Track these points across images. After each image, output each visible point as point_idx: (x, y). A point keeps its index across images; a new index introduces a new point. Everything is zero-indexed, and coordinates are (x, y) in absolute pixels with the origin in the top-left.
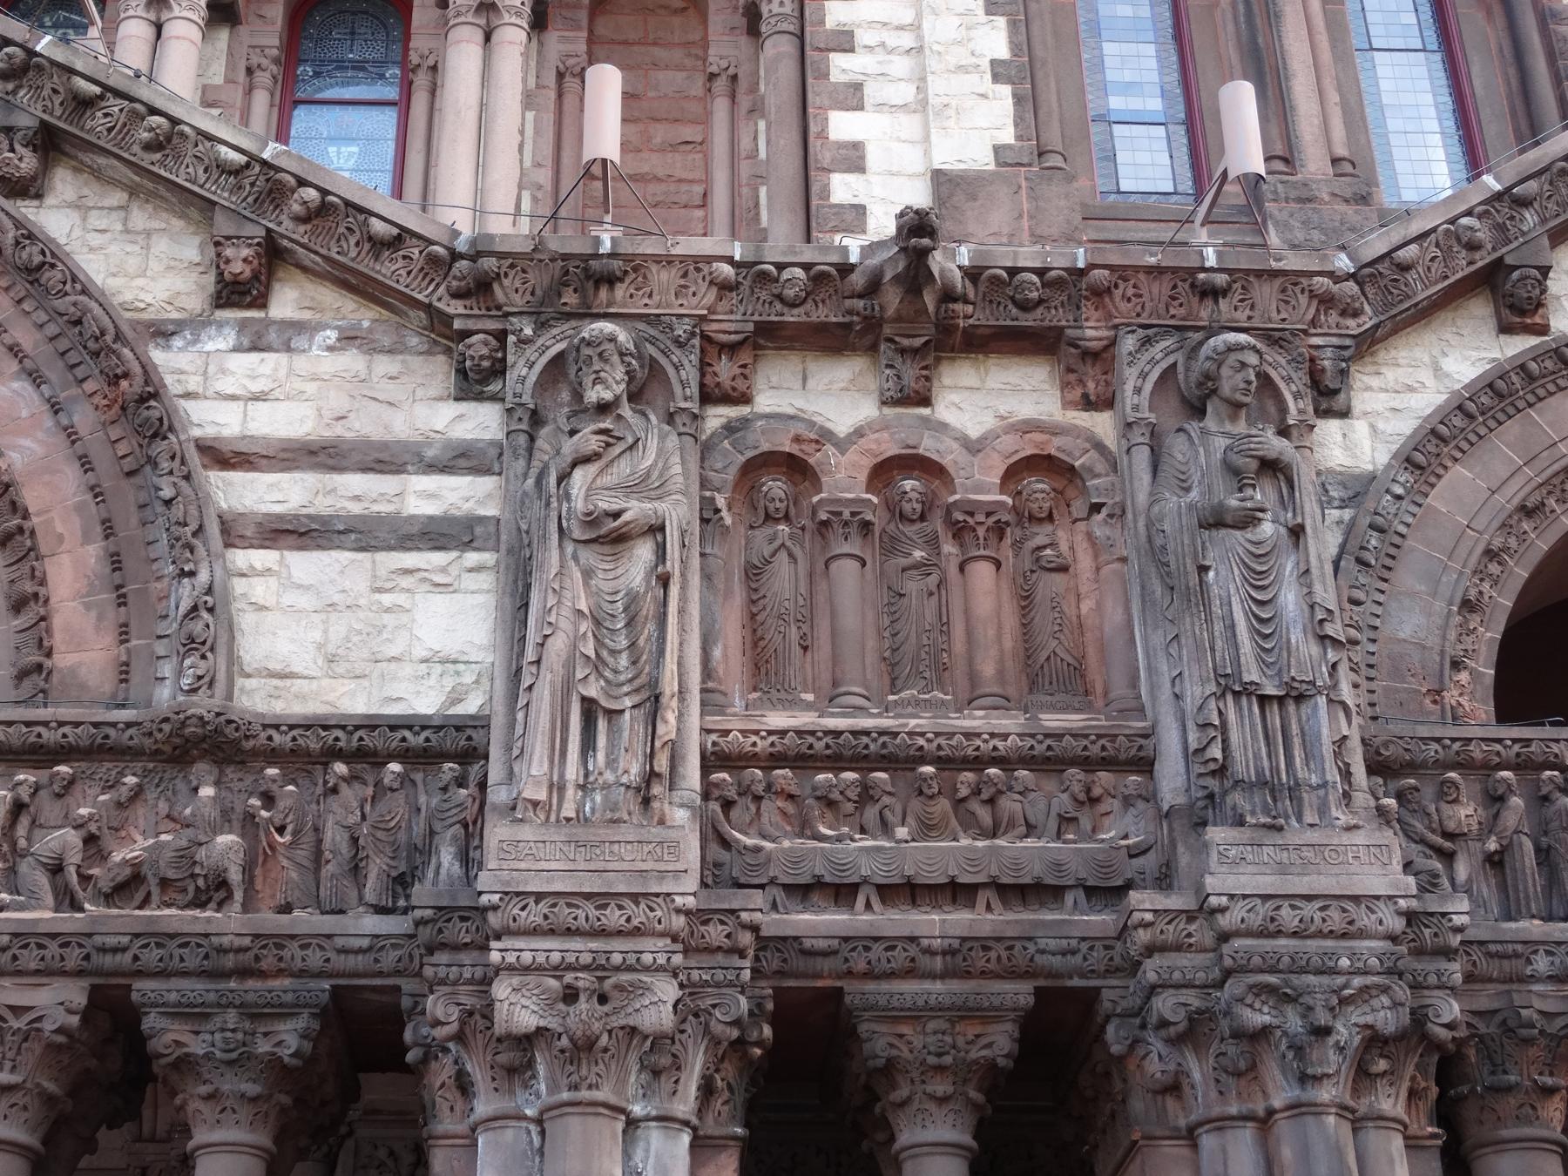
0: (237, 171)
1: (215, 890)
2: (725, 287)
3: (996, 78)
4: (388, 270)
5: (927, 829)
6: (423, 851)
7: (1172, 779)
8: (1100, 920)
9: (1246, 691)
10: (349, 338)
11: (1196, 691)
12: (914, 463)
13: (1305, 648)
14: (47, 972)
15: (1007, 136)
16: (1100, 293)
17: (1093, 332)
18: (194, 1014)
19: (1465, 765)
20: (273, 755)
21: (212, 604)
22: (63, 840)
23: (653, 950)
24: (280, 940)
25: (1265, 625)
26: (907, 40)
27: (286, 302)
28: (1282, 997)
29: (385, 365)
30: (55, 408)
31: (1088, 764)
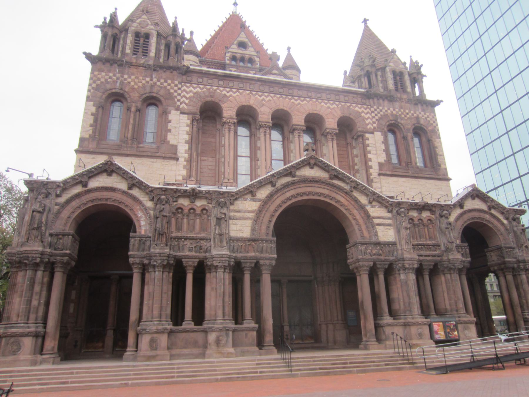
0: (371, 192)
1: (380, 255)
2: (409, 205)
3: (384, 151)
4: (384, 202)
5: (426, 251)
6: (393, 253)
7: (443, 248)
8: (439, 258)
9: (450, 242)
10: (379, 207)
11: (446, 242)
12: (420, 219)
13: (453, 238)
14: (371, 261)
15: (385, 159)
16: (435, 207)
17: (434, 209)
18: (380, 265)
19: (460, 246)
20: (382, 244)
21: (376, 232)
22: (369, 251)
23: (415, 262)
24: (386, 259)
25: (450, 236)
26: (374, 146)
27: (374, 203)
28: (453, 265)
29: (382, 209)
30: (359, 213)
31: (436, 246)
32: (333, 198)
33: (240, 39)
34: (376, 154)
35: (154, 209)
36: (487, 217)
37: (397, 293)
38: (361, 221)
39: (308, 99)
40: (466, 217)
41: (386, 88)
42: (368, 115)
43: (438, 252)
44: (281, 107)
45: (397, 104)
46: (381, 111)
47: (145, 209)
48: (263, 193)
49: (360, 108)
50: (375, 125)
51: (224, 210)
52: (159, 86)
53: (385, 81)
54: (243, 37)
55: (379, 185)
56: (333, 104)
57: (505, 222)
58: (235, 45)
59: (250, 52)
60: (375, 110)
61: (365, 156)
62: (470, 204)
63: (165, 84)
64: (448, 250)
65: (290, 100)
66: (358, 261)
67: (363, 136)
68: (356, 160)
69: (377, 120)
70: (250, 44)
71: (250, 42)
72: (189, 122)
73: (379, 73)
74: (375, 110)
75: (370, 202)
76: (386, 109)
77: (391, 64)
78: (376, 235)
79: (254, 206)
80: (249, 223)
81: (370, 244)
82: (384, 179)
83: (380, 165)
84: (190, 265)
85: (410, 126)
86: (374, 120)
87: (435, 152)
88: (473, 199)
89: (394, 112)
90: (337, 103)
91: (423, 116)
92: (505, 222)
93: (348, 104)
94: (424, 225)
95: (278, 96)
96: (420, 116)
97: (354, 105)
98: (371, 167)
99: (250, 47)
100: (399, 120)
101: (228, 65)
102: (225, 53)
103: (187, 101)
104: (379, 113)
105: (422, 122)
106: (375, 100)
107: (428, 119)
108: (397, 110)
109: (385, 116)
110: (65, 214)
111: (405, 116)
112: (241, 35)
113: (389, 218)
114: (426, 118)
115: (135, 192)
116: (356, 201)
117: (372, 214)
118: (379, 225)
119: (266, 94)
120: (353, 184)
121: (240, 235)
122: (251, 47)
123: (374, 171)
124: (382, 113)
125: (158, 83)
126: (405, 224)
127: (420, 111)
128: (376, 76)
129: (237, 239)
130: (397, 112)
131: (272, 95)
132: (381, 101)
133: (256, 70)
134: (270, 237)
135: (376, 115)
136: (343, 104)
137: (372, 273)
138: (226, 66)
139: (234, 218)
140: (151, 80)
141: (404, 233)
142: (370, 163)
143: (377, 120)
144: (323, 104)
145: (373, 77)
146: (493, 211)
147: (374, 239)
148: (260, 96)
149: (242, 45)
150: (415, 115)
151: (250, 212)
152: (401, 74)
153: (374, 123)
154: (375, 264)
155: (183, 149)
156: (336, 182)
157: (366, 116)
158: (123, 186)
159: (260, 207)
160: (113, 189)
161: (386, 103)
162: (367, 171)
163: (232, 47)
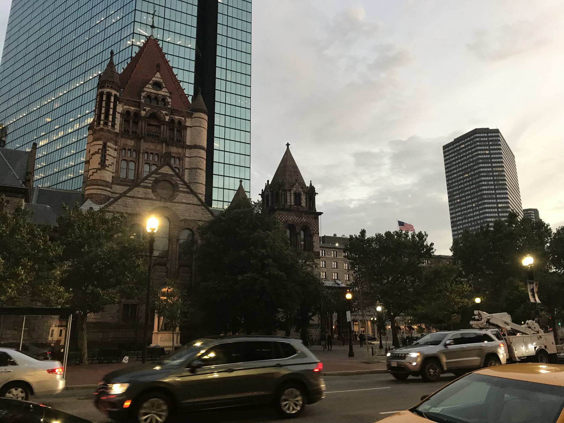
33: (154, 79)
54: (158, 77)
58: (150, 84)
59: (164, 92)
99: (164, 87)
101: (143, 104)
102: (141, 92)
112: (156, 76)
149: (157, 85)
163: (147, 86)
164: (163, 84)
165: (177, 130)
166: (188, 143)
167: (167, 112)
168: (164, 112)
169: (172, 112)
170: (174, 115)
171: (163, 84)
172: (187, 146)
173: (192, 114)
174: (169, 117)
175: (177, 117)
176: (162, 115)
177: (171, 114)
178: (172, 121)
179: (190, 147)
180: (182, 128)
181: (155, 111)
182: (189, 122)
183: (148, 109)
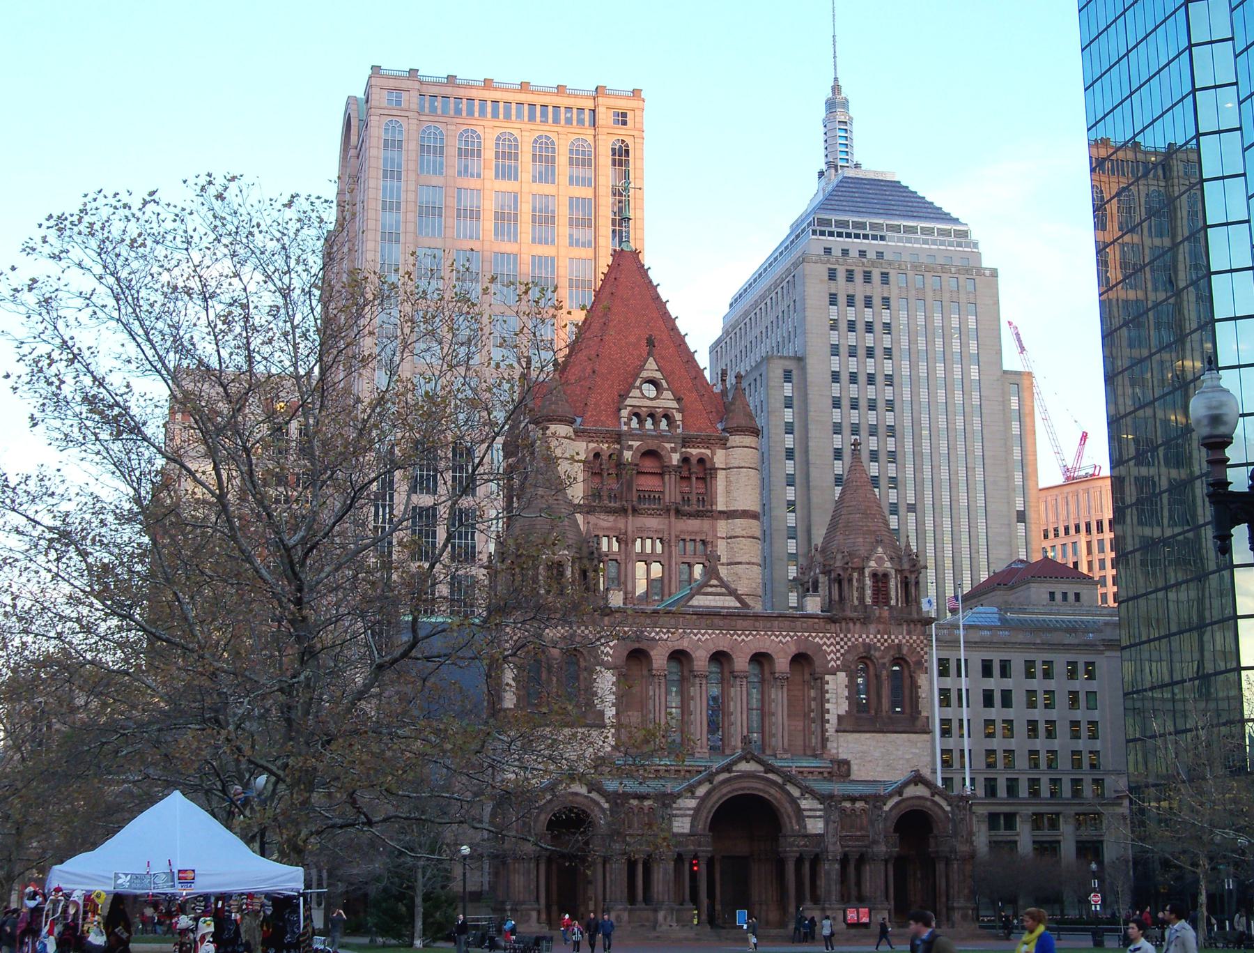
32: (766, 792)
33: (644, 374)
34: (837, 703)
35: (611, 810)
36: (929, 803)
37: (822, 882)
38: (792, 814)
39: (754, 633)
40: (903, 805)
41: (862, 599)
42: (832, 647)
43: (867, 843)
44: (721, 649)
45: (872, 628)
46: (849, 640)
47: (603, 810)
48: (701, 791)
49: (821, 639)
50: (838, 662)
51: (669, 811)
52: (579, 635)
53: (862, 589)
55: (835, 745)
56: (786, 636)
57: (948, 808)
59: (668, 401)
60: (842, 639)
61: (822, 706)
62: (911, 791)
63: (587, 632)
64: (875, 842)
65: (732, 636)
66: (785, 852)
67: (822, 679)
68: (813, 705)
69: (842, 655)
70: (665, 385)
71: (665, 378)
72: (614, 679)
73: (855, 575)
74: (842, 639)
75: (802, 795)
76: (856, 636)
77: (872, 564)
78: (805, 827)
79: (692, 803)
80: (688, 819)
81: (799, 836)
82: (844, 737)
83: (839, 717)
84: (640, 857)
85: (885, 660)
86: (838, 655)
87: (917, 693)
88: (916, 785)
89: (868, 640)
90: (792, 634)
91: (908, 641)
92: (948, 808)
93: (806, 634)
94: (856, 816)
95: (717, 632)
96: (904, 641)
97: (814, 634)
98: (828, 721)
100: (872, 652)
103: (611, 652)
104: (846, 643)
105: (905, 650)
106: (844, 624)
107: (915, 645)
108: (871, 636)
109: (854, 646)
110: (542, 817)
111: (882, 644)
113: (820, 810)
114: (911, 645)
115: (594, 795)
116: (789, 794)
117: (803, 807)
118: (809, 817)
119: (703, 631)
120: (787, 778)
121: (681, 831)
122: (667, 390)
123: (831, 727)
124: (849, 644)
125: (579, 631)
126: (835, 816)
127: (905, 633)
128: (850, 580)
129: (682, 835)
130: (871, 640)
131: (710, 632)
132: (851, 625)
133: (676, 440)
134: (707, 833)
135: (842, 647)
136: (799, 634)
137: (799, 861)
138: (623, 438)
139: (676, 816)
140: (571, 628)
141: (832, 826)
142: (827, 716)
143: (842, 655)
144: (773, 637)
145: (845, 585)
146: (937, 798)
147: (803, 830)
148: (696, 635)
150: (896, 641)
151: (689, 809)
152: (886, 576)
153: (838, 659)
154: (801, 855)
155: (610, 712)
156: (770, 776)
157: (829, 650)
158: (583, 790)
159: (698, 804)
160: (577, 794)
161: (858, 625)
162: (823, 726)
164: (663, 382)
165: (697, 478)
166: (719, 508)
167: (673, 445)
168: (668, 446)
169: (686, 441)
170: (689, 447)
171: (663, 382)
172: (720, 512)
173: (727, 440)
174: (682, 453)
175: (694, 451)
176: (663, 453)
177: (683, 446)
178: (685, 460)
179: (730, 515)
180: (706, 471)
181: (652, 444)
182: (720, 458)
183: (636, 444)
